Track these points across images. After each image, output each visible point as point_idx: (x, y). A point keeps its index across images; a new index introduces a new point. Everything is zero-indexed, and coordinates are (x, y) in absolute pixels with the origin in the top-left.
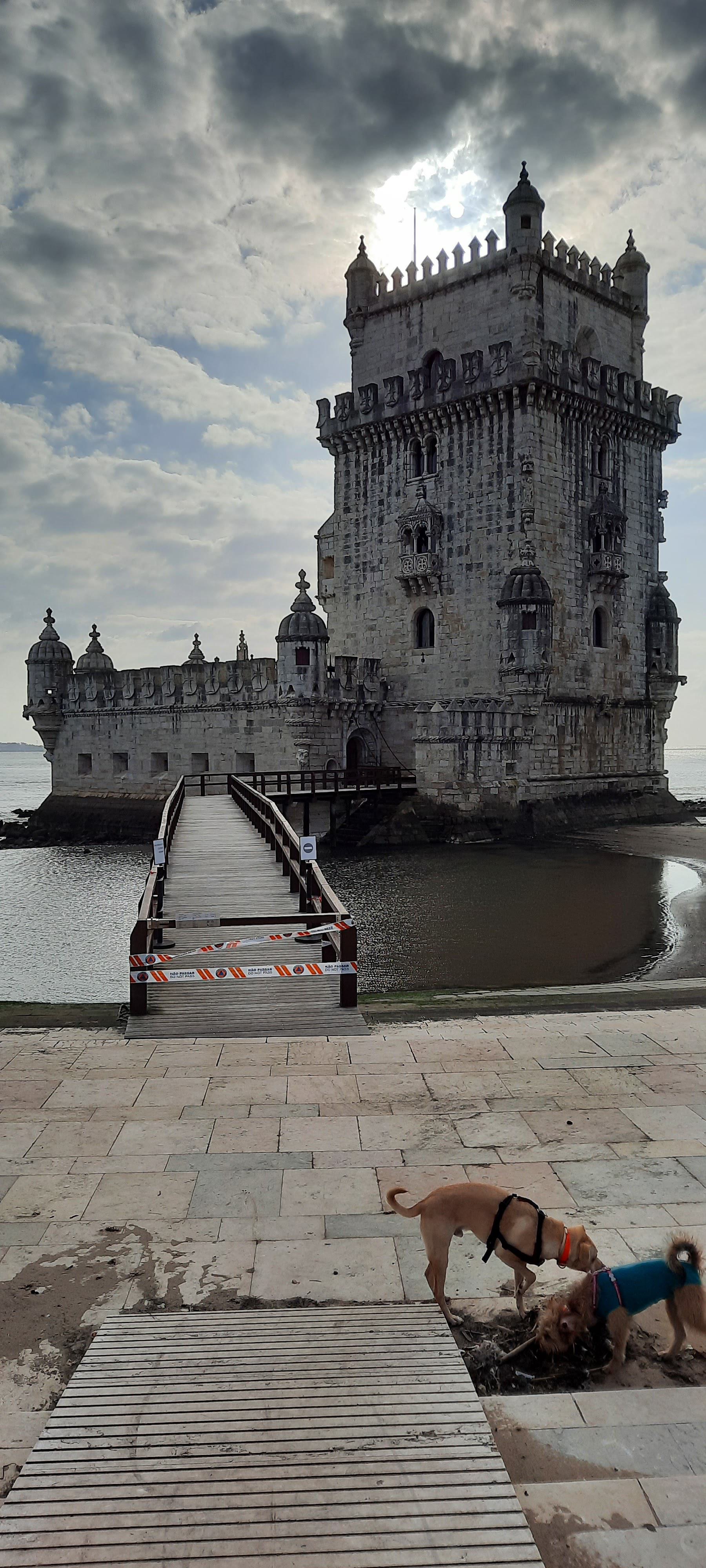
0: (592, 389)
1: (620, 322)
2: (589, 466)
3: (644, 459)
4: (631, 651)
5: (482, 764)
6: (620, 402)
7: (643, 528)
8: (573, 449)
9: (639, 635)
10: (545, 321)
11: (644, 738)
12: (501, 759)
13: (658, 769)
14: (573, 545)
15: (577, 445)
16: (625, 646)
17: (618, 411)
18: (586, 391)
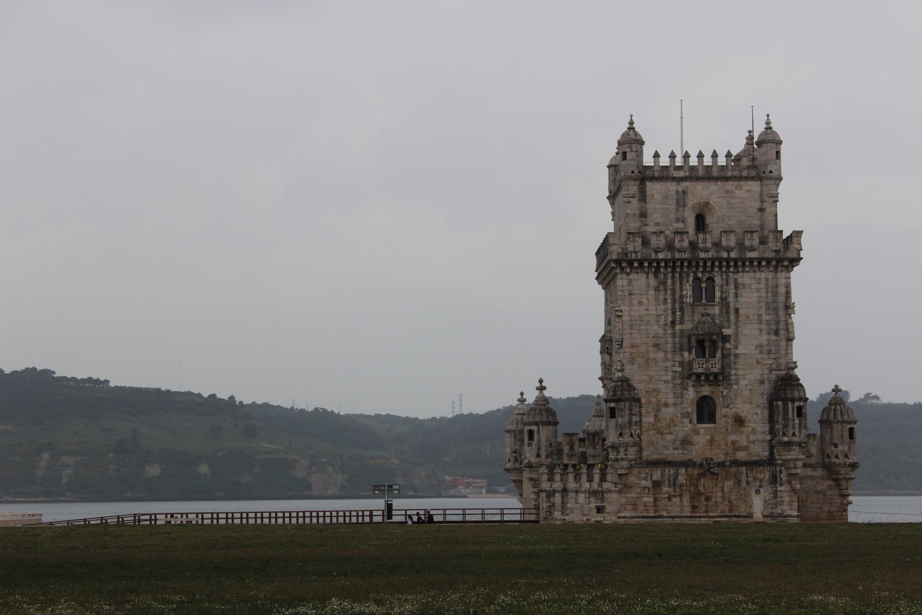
1: (745, 188)
2: (689, 300)
3: (764, 282)
5: (569, 505)
6: (718, 252)
7: (764, 332)
8: (669, 292)
9: (759, 412)
10: (649, 211)
12: (589, 503)
13: (789, 512)
14: (670, 356)
15: (673, 290)
16: (739, 421)
17: (713, 260)
18: (673, 254)
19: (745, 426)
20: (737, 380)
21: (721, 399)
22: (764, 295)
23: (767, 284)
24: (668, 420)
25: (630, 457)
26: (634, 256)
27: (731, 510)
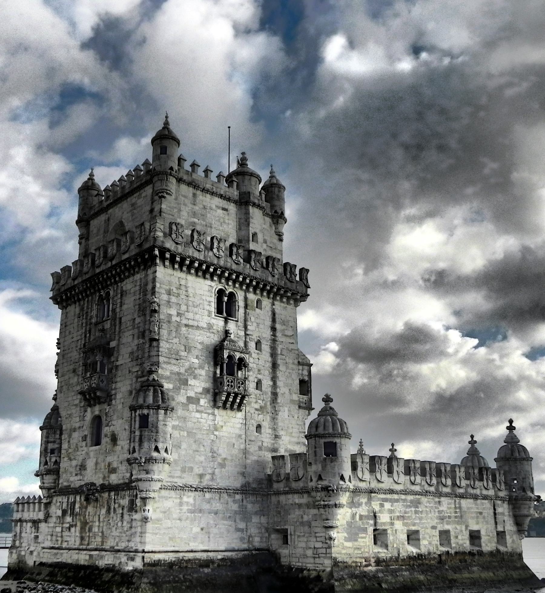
0: (86, 274)
3: (138, 284)
4: (118, 443)
5: (23, 535)
9: (127, 427)
10: (90, 246)
11: (126, 517)
14: (80, 380)
15: (87, 313)
16: (114, 439)
19: (117, 445)
20: (115, 394)
21: (105, 417)
22: (138, 297)
23: (140, 285)
24: (75, 444)
25: (46, 485)
26: (63, 289)
27: (103, 542)
